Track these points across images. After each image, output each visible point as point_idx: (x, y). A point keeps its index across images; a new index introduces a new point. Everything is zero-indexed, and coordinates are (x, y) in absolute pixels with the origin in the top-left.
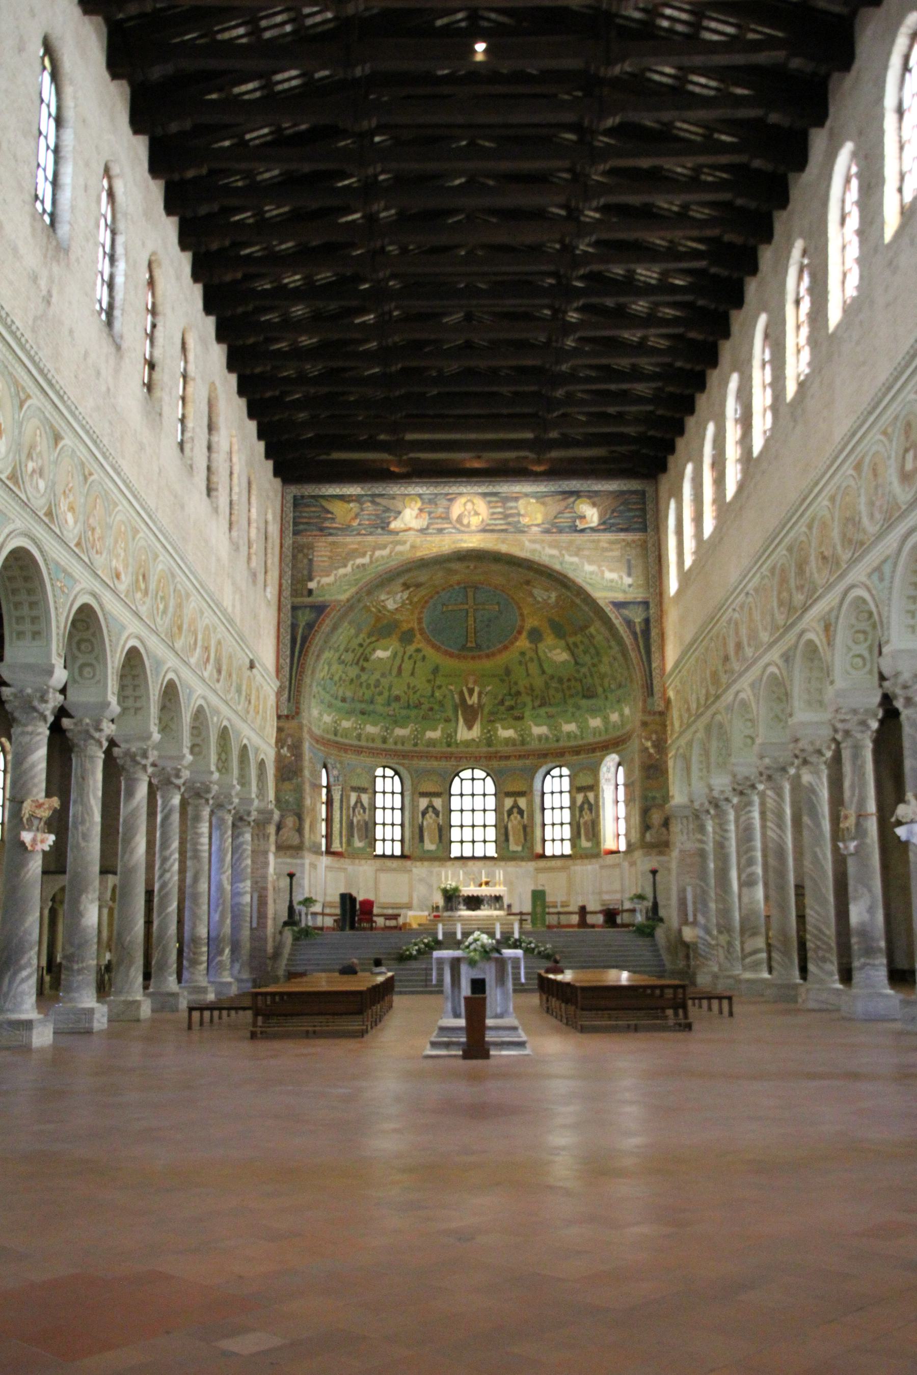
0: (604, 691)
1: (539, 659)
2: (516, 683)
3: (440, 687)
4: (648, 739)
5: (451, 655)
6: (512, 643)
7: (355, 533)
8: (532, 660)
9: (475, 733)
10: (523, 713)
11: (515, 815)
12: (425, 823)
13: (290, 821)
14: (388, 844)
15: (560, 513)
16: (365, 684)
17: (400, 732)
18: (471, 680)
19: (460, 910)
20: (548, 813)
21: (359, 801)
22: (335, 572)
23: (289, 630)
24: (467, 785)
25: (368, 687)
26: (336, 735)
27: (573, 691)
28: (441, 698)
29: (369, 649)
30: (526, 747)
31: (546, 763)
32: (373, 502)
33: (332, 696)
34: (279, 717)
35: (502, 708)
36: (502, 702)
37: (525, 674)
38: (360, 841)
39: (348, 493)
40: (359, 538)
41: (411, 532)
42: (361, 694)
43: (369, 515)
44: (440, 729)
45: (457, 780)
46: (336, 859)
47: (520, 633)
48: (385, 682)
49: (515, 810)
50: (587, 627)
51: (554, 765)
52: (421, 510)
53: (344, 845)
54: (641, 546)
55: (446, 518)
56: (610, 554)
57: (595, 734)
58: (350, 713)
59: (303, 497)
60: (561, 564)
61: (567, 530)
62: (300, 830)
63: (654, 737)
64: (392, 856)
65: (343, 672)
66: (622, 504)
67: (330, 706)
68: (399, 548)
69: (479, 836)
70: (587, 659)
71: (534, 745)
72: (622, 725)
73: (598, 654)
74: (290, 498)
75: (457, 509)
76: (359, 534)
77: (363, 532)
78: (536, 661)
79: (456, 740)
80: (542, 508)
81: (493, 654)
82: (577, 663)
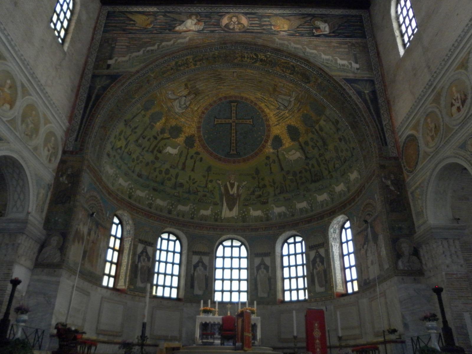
0: (330, 172)
1: (279, 160)
2: (263, 179)
3: (211, 181)
5: (220, 159)
6: (261, 151)
7: (149, 32)
8: (274, 162)
9: (235, 212)
12: (196, 274)
13: (55, 240)
14: (167, 290)
15: (301, 25)
17: (180, 207)
21: (144, 251)
22: (130, 54)
23: (87, 91)
25: (160, 172)
26: (130, 198)
31: (284, 231)
32: (165, 16)
33: (129, 168)
34: (64, 152)
36: (253, 193)
38: (142, 282)
39: (148, 10)
40: (151, 36)
41: (191, 32)
43: (161, 22)
44: (210, 209)
45: (221, 247)
47: (266, 142)
49: (262, 266)
50: (317, 122)
52: (199, 21)
53: (127, 286)
55: (218, 24)
56: (341, 50)
57: (322, 206)
59: (114, 12)
60: (304, 53)
61: (307, 35)
62: (62, 249)
63: (392, 177)
65: (140, 153)
66: (345, 22)
67: (126, 174)
68: (180, 41)
72: (349, 190)
73: (325, 144)
74: (105, 12)
75: (225, 21)
77: (155, 32)
79: (221, 217)
80: (288, 22)
82: (307, 158)
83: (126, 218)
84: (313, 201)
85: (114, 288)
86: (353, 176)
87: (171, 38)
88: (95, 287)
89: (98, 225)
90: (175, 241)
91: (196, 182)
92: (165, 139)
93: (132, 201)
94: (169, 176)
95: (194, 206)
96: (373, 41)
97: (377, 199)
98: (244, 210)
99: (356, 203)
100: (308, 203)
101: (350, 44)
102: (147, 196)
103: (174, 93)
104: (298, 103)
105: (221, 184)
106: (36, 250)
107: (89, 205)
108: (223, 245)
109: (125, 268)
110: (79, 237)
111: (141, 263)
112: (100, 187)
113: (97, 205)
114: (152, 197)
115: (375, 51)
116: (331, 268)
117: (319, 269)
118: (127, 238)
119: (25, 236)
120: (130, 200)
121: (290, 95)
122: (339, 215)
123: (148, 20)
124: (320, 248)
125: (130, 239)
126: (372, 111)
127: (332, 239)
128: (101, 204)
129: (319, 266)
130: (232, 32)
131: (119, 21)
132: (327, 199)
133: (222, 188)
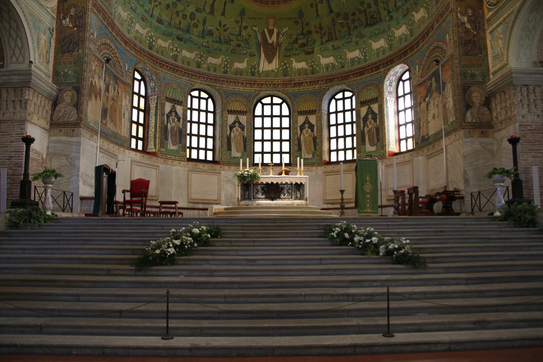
0: (389, 12)
2: (307, 24)
3: (246, 28)
4: (463, 15)
9: (274, 65)
10: (313, 49)
11: (307, 130)
12: (232, 135)
13: (68, 96)
14: (202, 153)
17: (211, 60)
18: (271, 21)
19: (259, 198)
20: (333, 129)
21: (173, 111)
28: (247, 37)
30: (316, 75)
31: (332, 86)
33: (145, 10)
36: (296, 41)
37: (316, 15)
38: (174, 145)
42: (177, 22)
44: (246, 61)
45: (259, 105)
46: (146, 156)
48: (199, 16)
49: (307, 126)
58: (166, 35)
62: (78, 106)
63: (470, 12)
64: (205, 161)
67: (144, 19)
69: (276, 148)
71: (323, 73)
72: (412, 33)
83: (149, 73)
84: (367, 49)
85: (144, 151)
86: (419, 15)
88: (122, 149)
89: (116, 79)
90: (207, 99)
91: (228, 28)
93: (153, 52)
94: (196, 21)
95: (227, 58)
97: (448, 40)
98: (286, 62)
99: (420, 48)
100: (360, 51)
102: (171, 47)
106: (48, 107)
107: (102, 55)
108: (262, 103)
109: (153, 130)
110: (94, 92)
111: (171, 124)
112: (114, 34)
113: (112, 55)
114: (176, 48)
116: (384, 125)
117: (370, 127)
118: (152, 96)
119: (32, 91)
120: (151, 51)
122: (397, 64)
124: (373, 103)
125: (156, 97)
127: (387, 93)
128: (117, 55)
129: (370, 123)
132: (384, 46)
133: (259, 35)
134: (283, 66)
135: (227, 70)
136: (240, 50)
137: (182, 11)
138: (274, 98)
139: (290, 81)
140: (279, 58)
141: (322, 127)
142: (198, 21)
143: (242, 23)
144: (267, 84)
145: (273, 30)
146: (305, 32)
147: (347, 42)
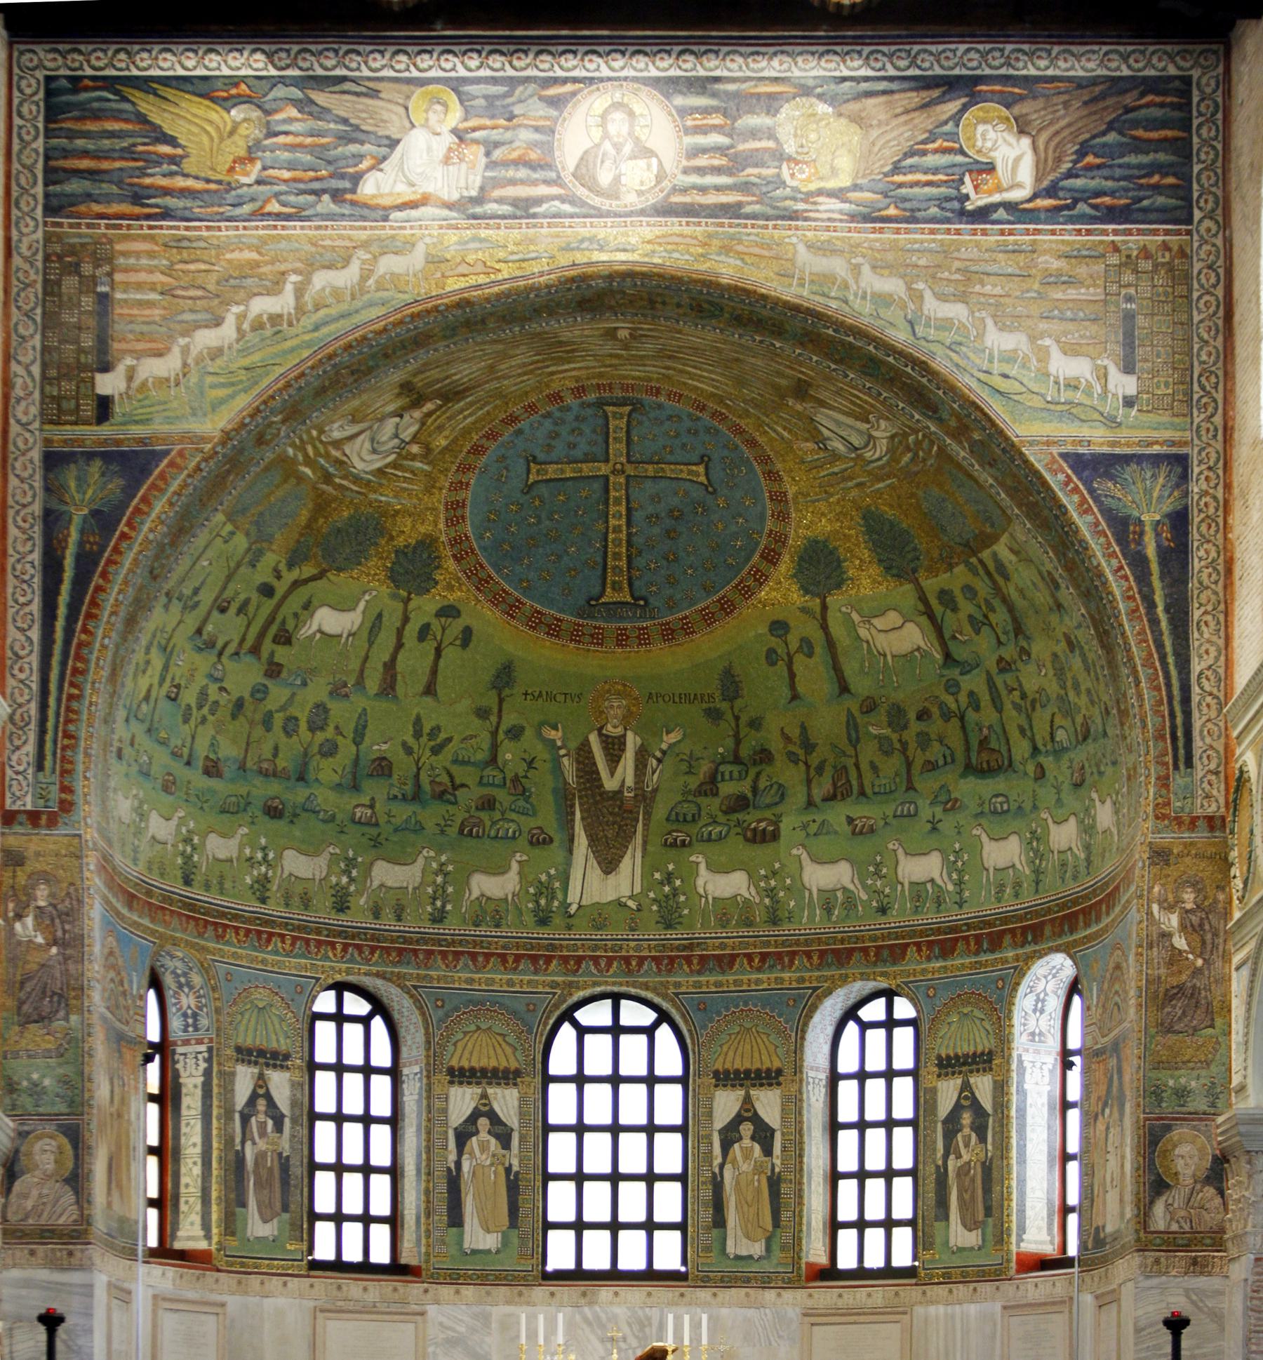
2: (755, 724)
3: (515, 733)
10: (776, 823)
11: (747, 1147)
16: (278, 719)
24: (598, 1046)
25: (290, 726)
27: (935, 753)
29: (295, 602)
30: (786, 929)
35: (712, 805)
36: (710, 786)
40: (259, 230)
42: (267, 752)
44: (515, 867)
45: (567, 1033)
50: (988, 540)
51: (870, 986)
54: (1170, 268)
56: (1072, 293)
60: (911, 323)
68: (389, 264)
70: (983, 646)
71: (810, 922)
76: (259, 214)
78: (819, 650)
81: (687, 629)
82: (948, 656)
87: (347, 243)
91: (449, 740)
92: (306, 581)
94: (330, 733)
95: (443, 858)
96: (1219, 241)
98: (671, 867)
101: (1114, 260)
103: (354, 421)
104: (903, 454)
105: (559, 743)
108: (575, 1024)
115: (1220, 292)
121: (868, 422)
123: (232, 133)
126: (1160, 609)
130: (608, 214)
131: (106, 143)
133: (565, 761)
134: (662, 883)
135: (444, 906)
136: (494, 823)
137: (283, 709)
138: (624, 1003)
139: (685, 948)
140: (644, 850)
141: (801, 1136)
142: (337, 728)
143: (500, 717)
144: (596, 960)
145: (621, 741)
146: (744, 752)
147: (902, 816)
